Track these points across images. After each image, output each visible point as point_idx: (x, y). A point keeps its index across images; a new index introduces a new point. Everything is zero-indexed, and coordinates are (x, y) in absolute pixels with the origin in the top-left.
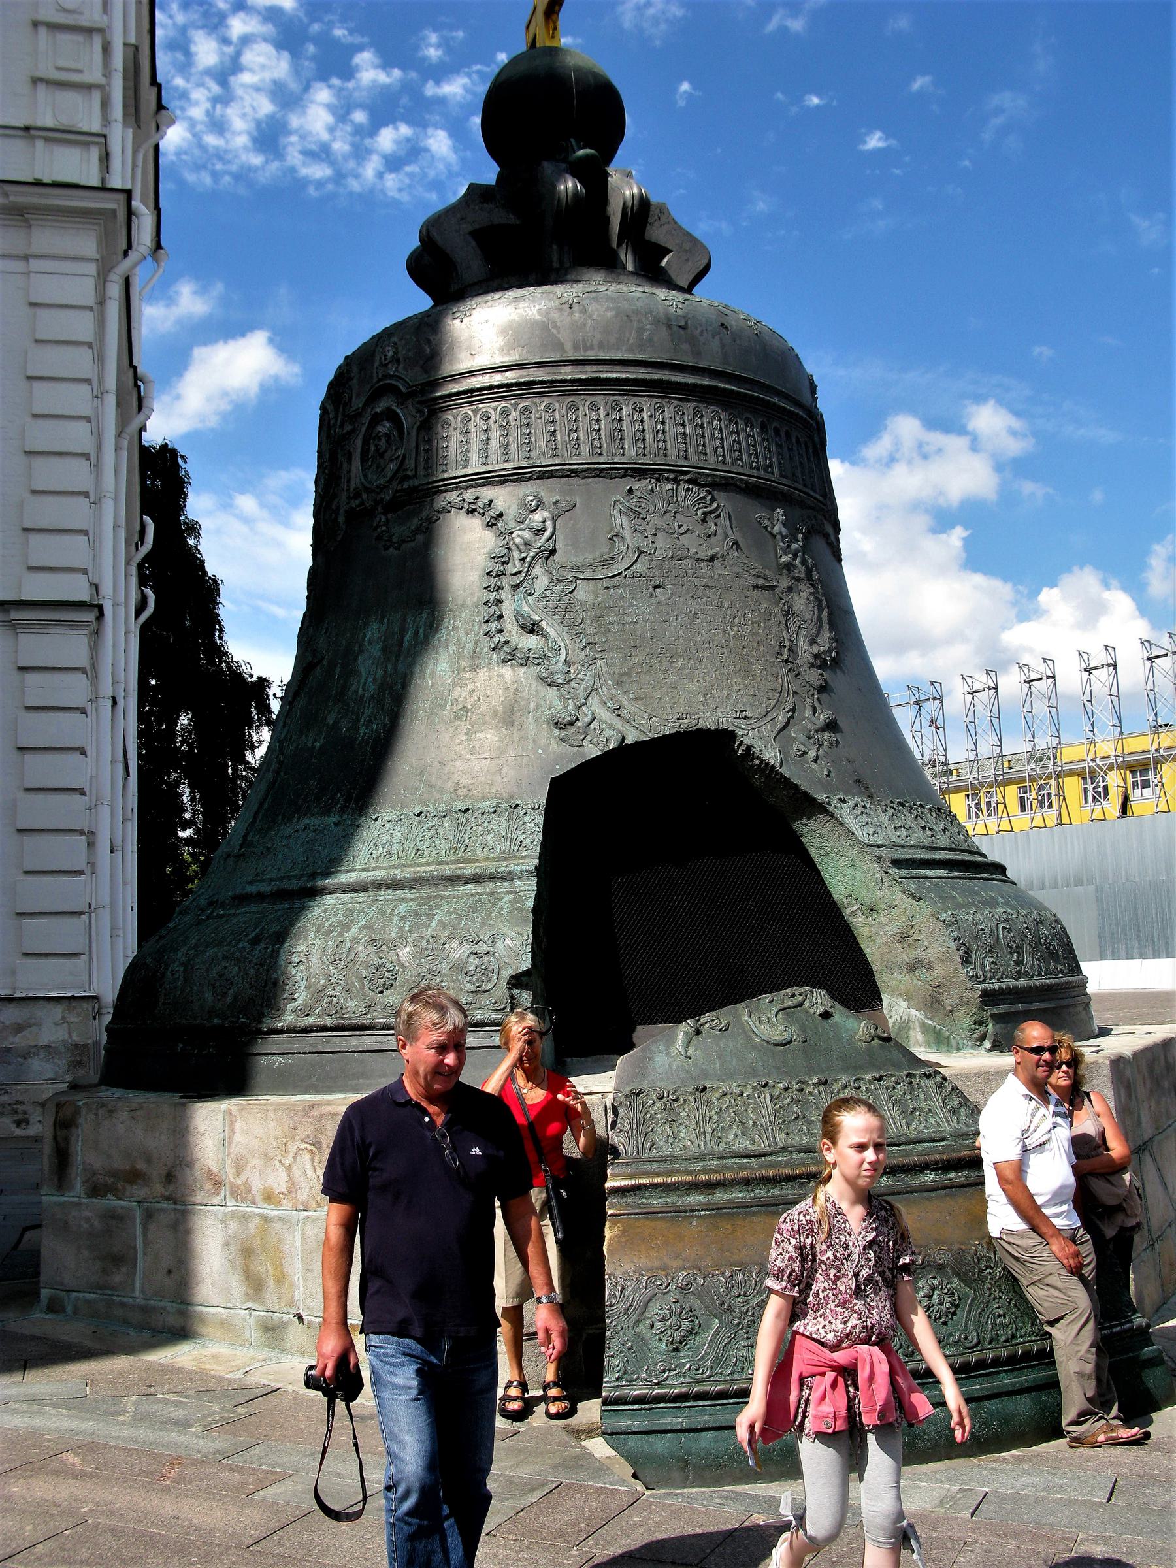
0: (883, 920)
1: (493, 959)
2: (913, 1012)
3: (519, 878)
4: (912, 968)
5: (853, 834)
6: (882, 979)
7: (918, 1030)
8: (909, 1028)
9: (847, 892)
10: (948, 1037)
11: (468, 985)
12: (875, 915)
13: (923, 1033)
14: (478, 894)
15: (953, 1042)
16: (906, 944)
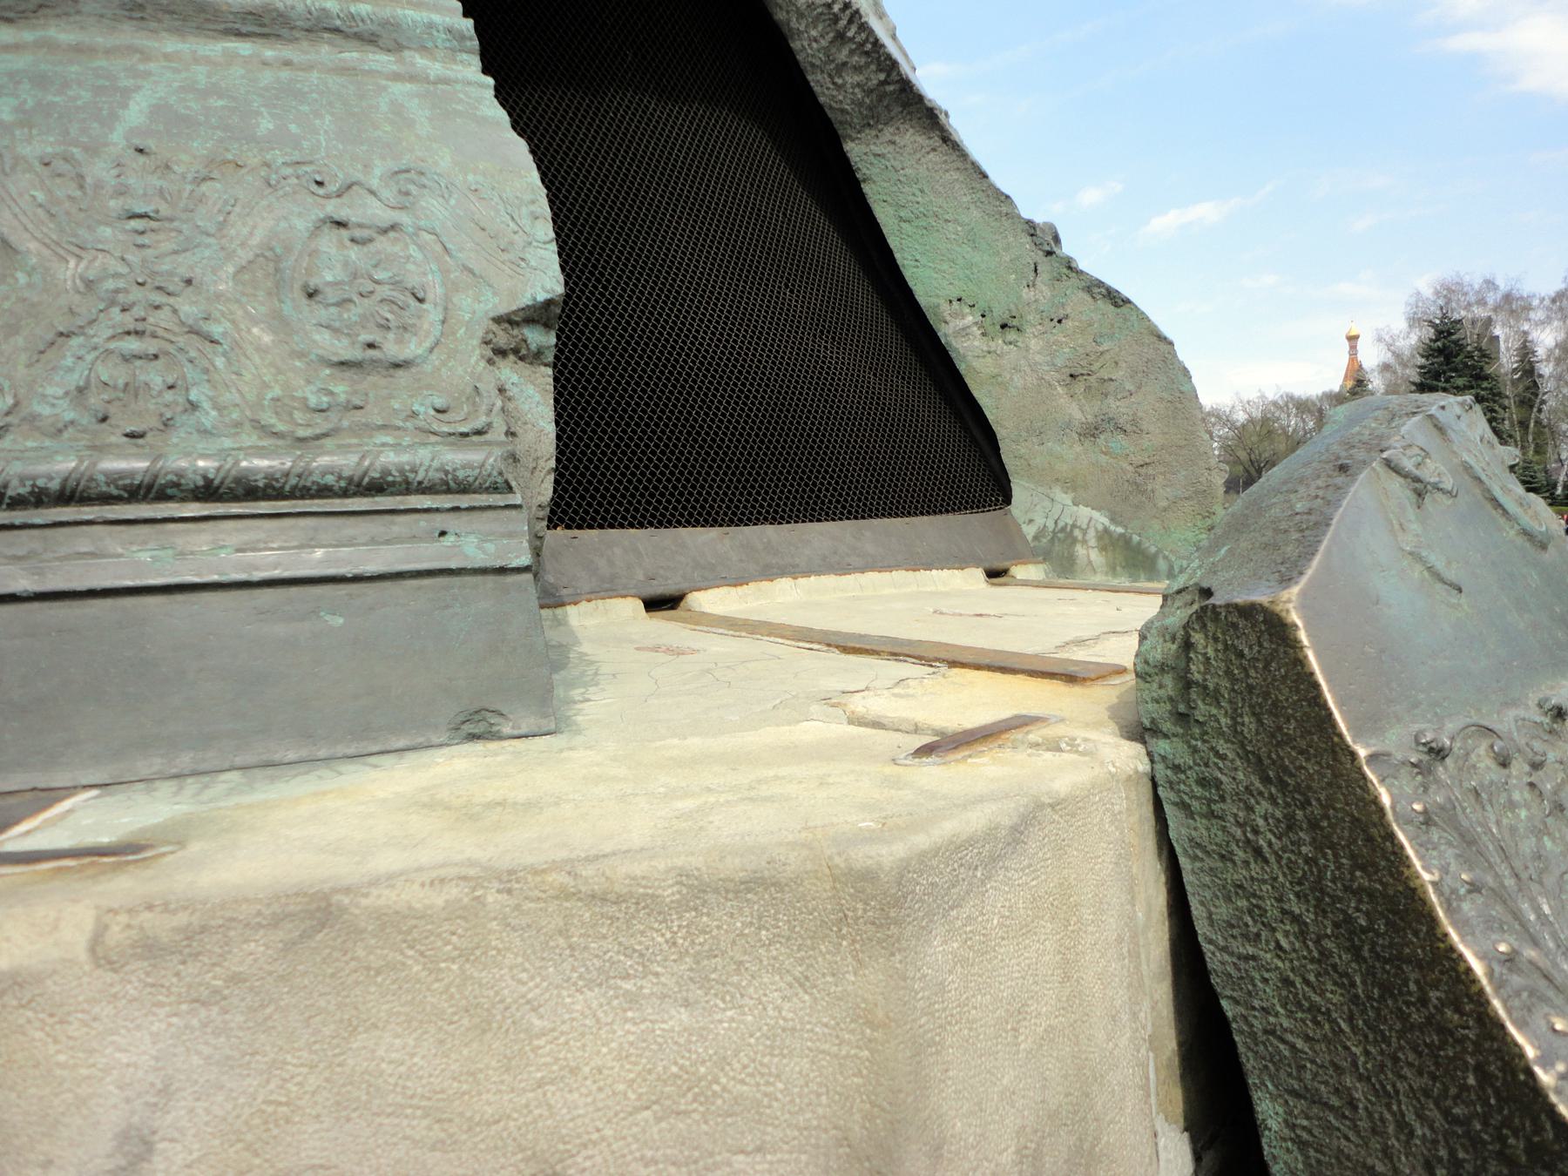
0: (1034, 344)
1: (413, 250)
2: (1084, 513)
3: (423, 49)
4: (1091, 432)
5: (985, 176)
6: (1011, 453)
7: (1093, 542)
8: (1075, 541)
9: (955, 294)
10: (1156, 555)
11: (323, 338)
12: (1011, 335)
13: (1103, 549)
14: (287, 63)
15: (1162, 565)
16: (1079, 387)
